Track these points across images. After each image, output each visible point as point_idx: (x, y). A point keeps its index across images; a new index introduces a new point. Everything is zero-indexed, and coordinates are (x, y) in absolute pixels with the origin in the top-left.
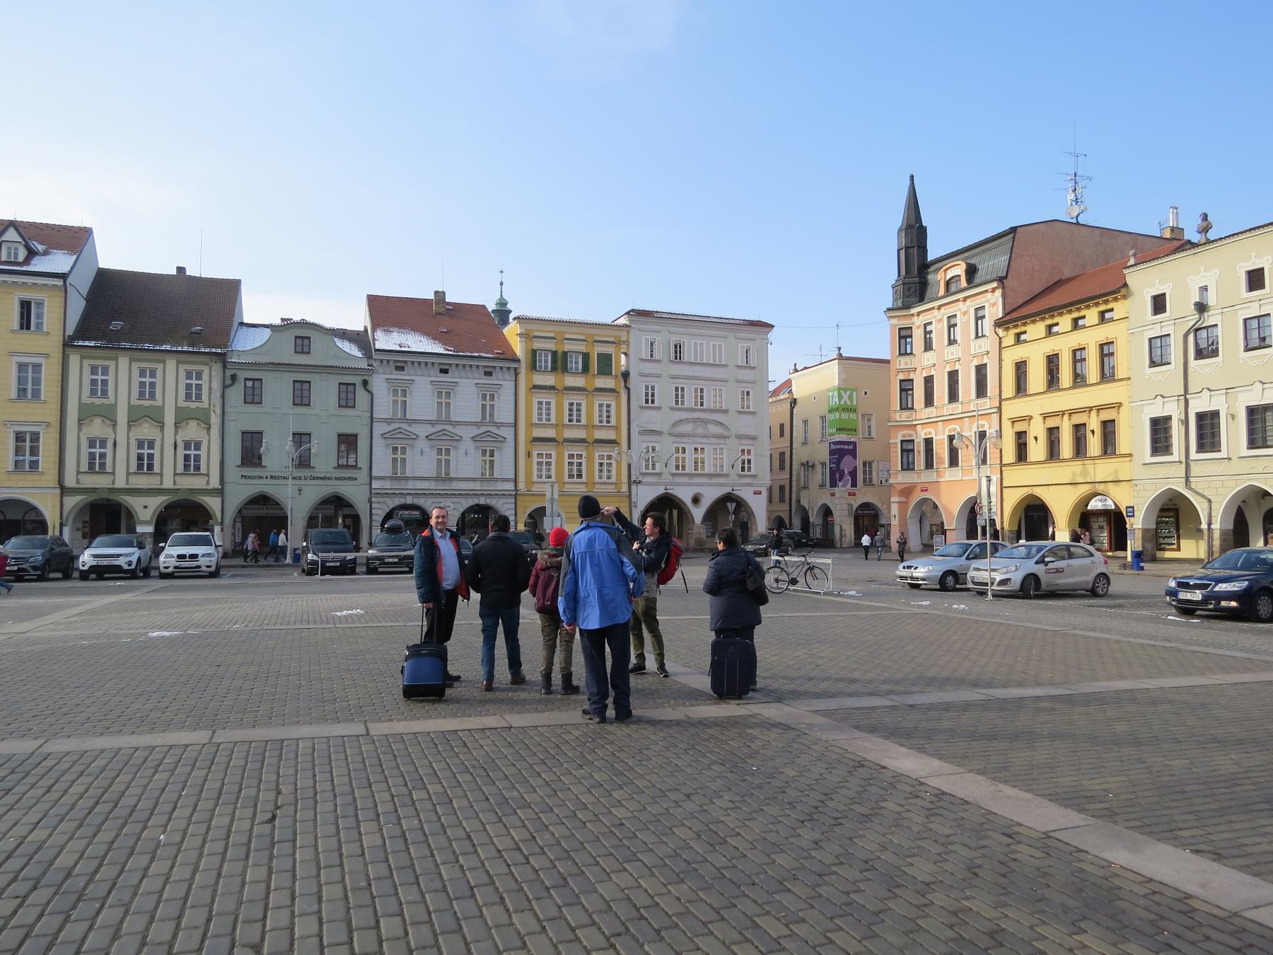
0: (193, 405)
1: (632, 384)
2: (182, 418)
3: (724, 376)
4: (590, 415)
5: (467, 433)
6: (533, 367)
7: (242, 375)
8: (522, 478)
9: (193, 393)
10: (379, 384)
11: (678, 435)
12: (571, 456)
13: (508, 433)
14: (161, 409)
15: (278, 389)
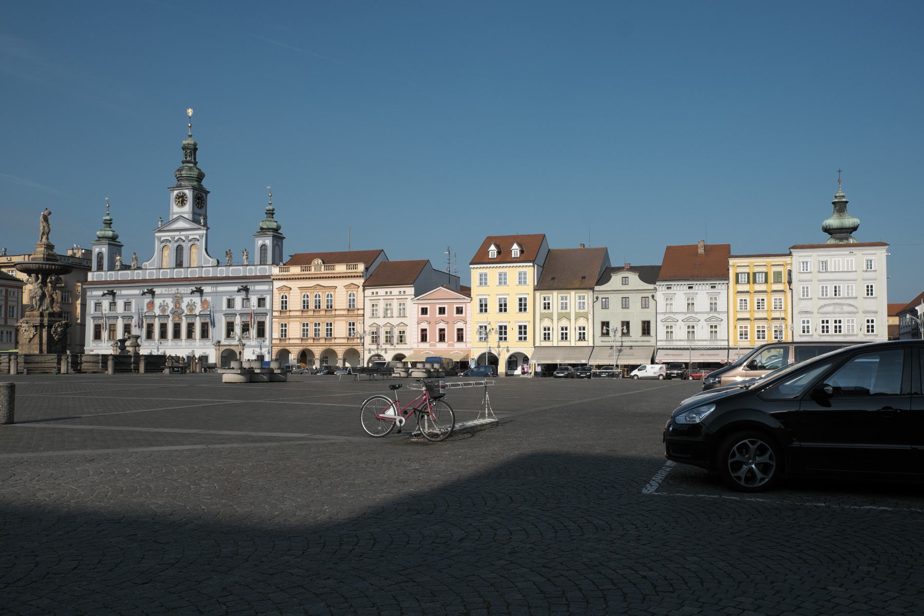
0: (582, 311)
1: (793, 286)
2: (578, 316)
3: (854, 278)
4: (752, 305)
5: (702, 317)
6: (737, 282)
7: (600, 296)
8: (731, 339)
9: (582, 306)
10: (659, 296)
11: (823, 313)
12: (758, 327)
13: (724, 317)
14: (569, 313)
15: (615, 301)
